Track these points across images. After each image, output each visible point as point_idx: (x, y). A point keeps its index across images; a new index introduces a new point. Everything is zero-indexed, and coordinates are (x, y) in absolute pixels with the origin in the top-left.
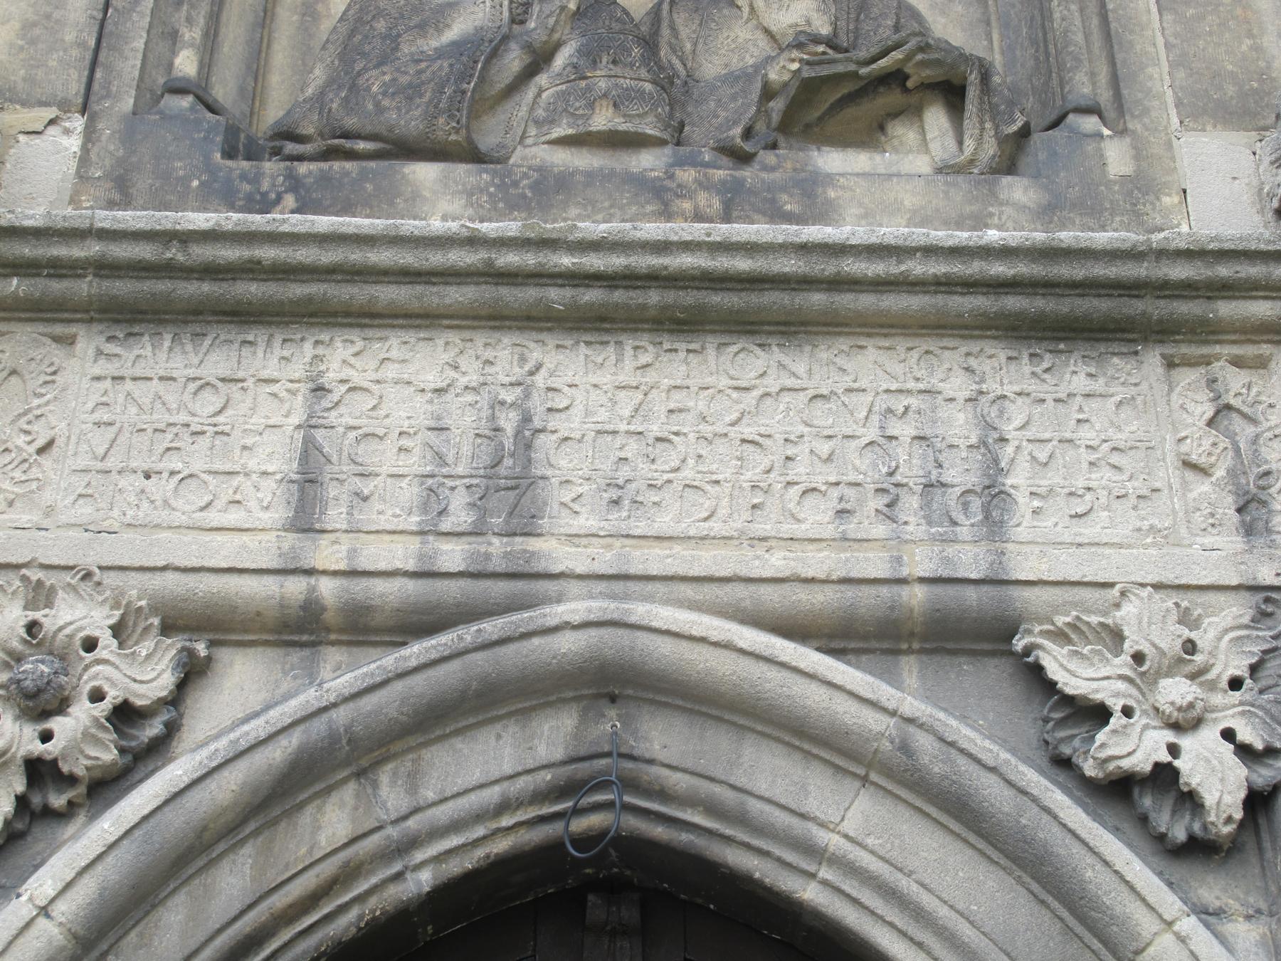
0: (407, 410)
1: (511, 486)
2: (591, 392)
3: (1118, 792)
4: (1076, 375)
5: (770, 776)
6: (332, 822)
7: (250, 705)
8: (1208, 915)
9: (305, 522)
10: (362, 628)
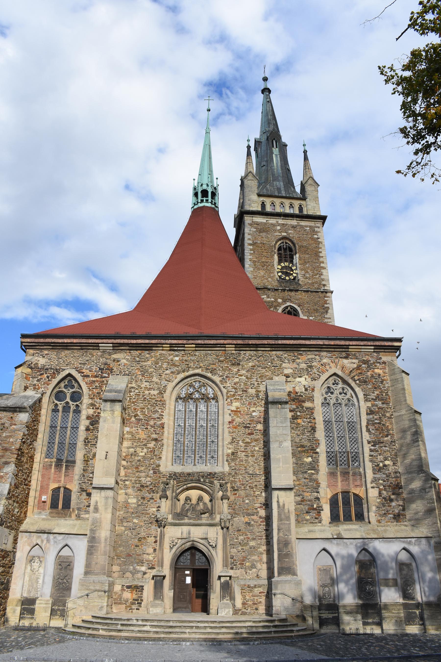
0: (185, 530)
1: (189, 533)
2: (192, 529)
3: (211, 545)
4: (211, 528)
5: (198, 544)
6: (183, 546)
7: (180, 542)
8: (213, 550)
9: (182, 534)
10: (184, 539)
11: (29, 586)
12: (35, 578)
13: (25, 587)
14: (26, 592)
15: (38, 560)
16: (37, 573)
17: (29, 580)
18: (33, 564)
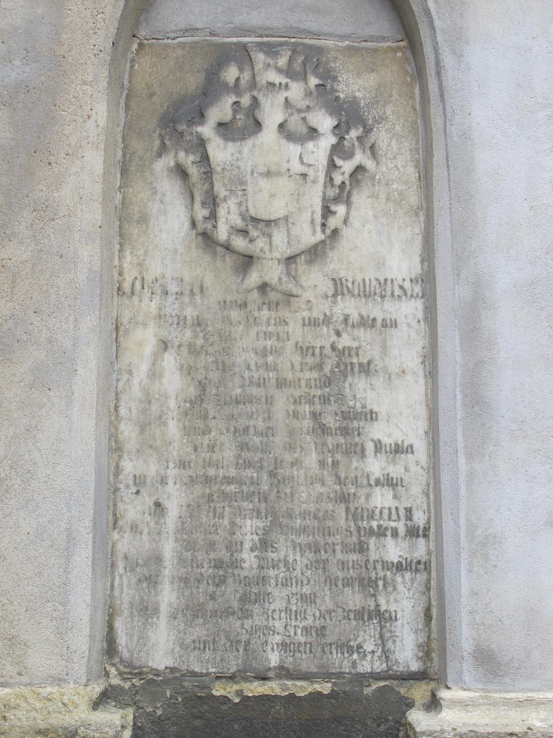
11: (211, 493)
12: (289, 358)
13: (133, 509)
14: (167, 596)
15: (296, 91)
16: (314, 281)
17: (195, 407)
18: (220, 152)
